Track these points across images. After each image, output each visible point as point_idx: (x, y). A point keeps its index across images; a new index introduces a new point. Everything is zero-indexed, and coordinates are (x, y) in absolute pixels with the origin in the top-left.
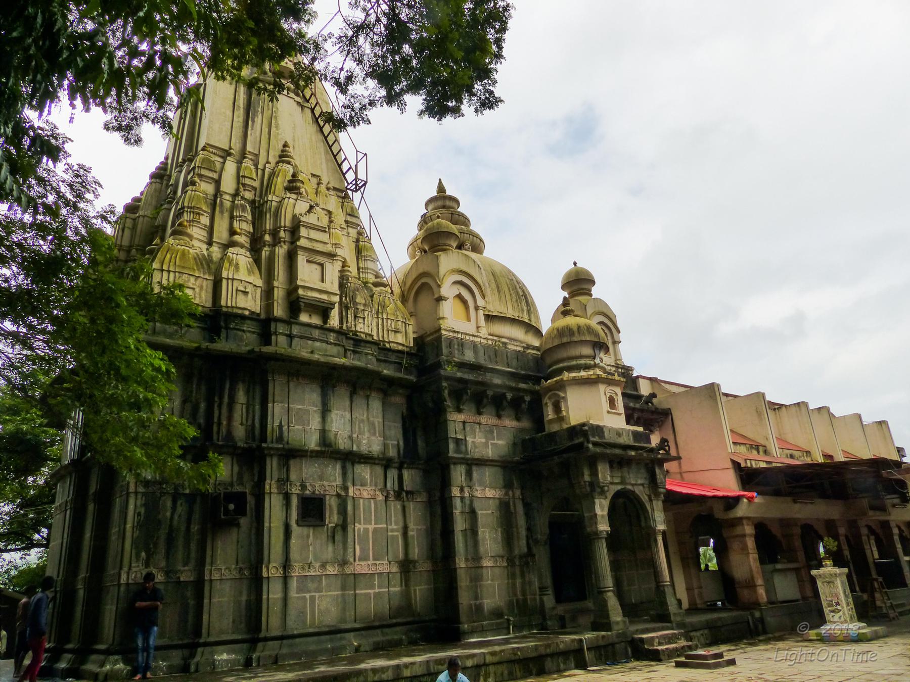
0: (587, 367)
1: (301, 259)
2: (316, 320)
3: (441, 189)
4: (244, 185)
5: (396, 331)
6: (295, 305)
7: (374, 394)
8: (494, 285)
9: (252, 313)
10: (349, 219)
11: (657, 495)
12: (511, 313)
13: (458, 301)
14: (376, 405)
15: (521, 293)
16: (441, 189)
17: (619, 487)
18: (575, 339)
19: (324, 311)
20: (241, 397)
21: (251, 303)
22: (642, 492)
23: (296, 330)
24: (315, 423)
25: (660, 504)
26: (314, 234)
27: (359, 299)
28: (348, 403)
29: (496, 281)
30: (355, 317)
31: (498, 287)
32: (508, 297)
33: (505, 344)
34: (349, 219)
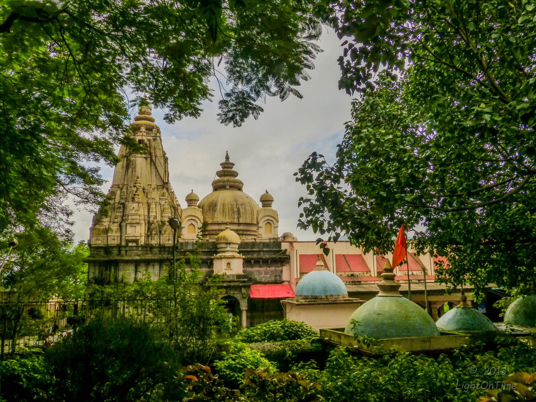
0: (223, 252)
1: (128, 227)
2: (134, 244)
3: (227, 158)
4: (122, 198)
5: (169, 240)
6: (128, 241)
7: (156, 264)
8: (222, 210)
9: (117, 244)
10: (162, 197)
11: (244, 298)
12: (227, 220)
13: (192, 226)
14: (157, 267)
15: (235, 210)
16: (227, 158)
17: (226, 295)
18: (219, 242)
19: (136, 241)
20: (113, 270)
21: (116, 242)
22: (238, 296)
23: (128, 249)
24: (133, 276)
25: (246, 300)
26: (133, 217)
27: (154, 232)
28: (144, 268)
29: (223, 208)
30: (151, 239)
31: (223, 210)
32: (227, 214)
33: (208, 240)
34: (162, 197)
